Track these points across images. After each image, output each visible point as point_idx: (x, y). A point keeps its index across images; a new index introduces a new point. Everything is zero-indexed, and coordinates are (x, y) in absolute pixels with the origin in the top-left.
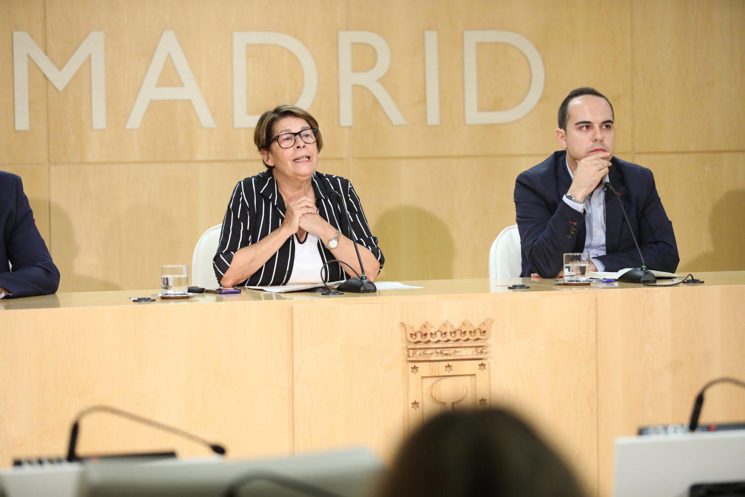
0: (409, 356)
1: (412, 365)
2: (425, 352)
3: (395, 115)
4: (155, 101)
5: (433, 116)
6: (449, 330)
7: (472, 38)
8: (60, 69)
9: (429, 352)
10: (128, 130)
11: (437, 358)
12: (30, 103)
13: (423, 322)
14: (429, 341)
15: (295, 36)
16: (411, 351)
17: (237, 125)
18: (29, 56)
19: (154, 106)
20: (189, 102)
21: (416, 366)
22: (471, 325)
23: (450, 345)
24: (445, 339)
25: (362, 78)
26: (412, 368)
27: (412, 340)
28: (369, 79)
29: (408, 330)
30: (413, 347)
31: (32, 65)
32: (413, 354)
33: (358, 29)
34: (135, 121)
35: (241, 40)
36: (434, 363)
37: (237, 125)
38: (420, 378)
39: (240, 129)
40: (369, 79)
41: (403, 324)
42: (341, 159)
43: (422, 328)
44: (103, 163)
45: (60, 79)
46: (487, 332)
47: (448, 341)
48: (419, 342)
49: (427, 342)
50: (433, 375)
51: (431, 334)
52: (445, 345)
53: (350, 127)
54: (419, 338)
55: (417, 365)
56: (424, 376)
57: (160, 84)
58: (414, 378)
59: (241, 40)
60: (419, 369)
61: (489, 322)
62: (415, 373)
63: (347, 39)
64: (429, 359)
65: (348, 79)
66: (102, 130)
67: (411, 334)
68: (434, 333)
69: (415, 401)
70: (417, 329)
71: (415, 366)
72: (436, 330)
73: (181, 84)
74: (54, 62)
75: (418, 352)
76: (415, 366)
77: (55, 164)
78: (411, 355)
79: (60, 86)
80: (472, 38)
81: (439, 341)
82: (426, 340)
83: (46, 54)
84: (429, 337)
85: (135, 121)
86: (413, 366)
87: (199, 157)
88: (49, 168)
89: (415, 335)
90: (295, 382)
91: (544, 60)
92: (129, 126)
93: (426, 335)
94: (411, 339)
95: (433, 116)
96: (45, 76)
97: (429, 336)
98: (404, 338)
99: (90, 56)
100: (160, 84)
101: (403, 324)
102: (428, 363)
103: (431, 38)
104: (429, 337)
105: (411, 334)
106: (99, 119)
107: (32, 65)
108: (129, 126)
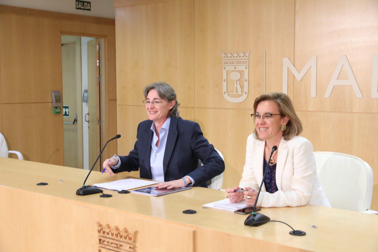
4: (337, 85)
6: (115, 232)
10: (325, 98)
11: (109, 248)
20: (351, 86)
21: (101, 249)
23: (115, 242)
24: (113, 237)
32: (100, 242)
34: (327, 95)
36: (108, 250)
39: (374, 98)
44: (315, 111)
55: (102, 249)
61: (133, 233)
66: (314, 97)
67: (99, 232)
68: (108, 232)
72: (109, 231)
85: (327, 95)
87: (355, 111)
92: (324, 97)
96: (294, 75)
97: (106, 234)
106: (313, 94)
108: (324, 97)
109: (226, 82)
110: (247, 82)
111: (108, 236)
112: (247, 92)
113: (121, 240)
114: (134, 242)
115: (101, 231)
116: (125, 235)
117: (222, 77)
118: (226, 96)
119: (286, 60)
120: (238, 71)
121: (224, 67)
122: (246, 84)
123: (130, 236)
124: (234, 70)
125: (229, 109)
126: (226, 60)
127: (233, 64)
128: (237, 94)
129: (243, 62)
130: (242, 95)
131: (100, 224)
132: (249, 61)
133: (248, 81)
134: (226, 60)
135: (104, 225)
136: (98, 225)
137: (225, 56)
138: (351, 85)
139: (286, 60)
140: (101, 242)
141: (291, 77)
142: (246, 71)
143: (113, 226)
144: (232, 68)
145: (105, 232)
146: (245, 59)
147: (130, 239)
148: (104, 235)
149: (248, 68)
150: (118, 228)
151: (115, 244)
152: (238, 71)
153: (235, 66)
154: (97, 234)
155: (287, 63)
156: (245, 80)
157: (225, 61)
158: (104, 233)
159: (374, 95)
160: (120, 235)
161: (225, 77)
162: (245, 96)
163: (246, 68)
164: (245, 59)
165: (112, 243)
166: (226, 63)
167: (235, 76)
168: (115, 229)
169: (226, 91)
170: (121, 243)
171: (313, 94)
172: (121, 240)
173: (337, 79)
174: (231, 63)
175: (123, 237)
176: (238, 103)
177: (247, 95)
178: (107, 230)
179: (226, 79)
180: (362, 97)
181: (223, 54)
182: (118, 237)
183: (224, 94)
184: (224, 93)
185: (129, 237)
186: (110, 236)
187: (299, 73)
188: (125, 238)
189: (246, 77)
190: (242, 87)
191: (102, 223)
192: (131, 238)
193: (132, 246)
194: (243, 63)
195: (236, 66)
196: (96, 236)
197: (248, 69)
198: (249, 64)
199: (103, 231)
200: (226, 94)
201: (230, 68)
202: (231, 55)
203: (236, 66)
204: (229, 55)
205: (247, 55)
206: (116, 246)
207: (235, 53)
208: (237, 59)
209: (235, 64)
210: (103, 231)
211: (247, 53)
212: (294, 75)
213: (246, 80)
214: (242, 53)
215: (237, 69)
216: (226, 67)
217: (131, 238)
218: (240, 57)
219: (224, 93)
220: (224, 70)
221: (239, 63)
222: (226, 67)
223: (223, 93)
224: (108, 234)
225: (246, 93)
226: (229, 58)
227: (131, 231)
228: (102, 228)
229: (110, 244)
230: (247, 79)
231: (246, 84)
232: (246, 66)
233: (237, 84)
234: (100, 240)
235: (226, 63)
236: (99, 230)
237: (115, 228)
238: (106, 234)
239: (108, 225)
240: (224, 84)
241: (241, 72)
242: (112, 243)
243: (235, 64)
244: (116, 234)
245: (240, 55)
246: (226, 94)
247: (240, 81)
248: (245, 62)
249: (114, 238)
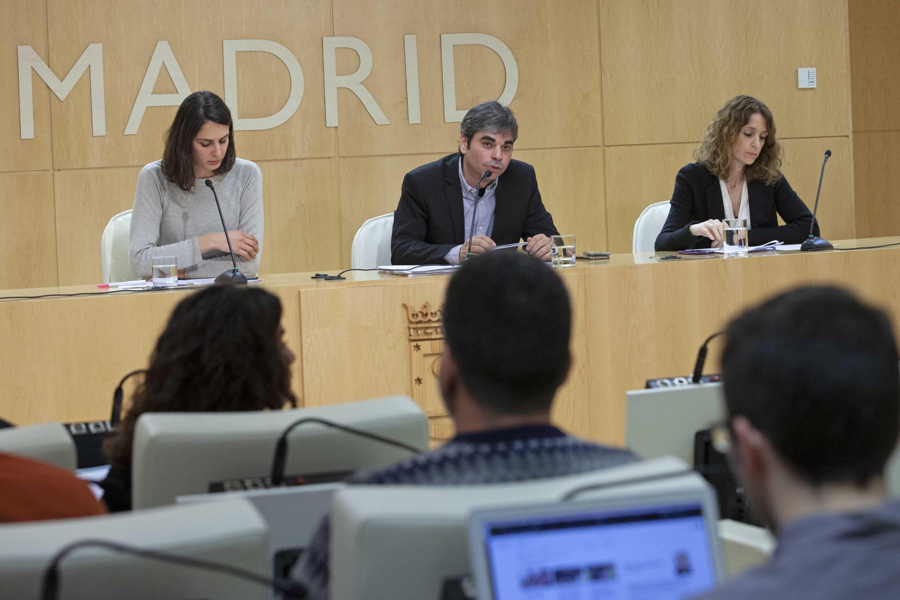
0: (410, 335)
1: (414, 344)
2: (426, 331)
3: (379, 116)
5: (415, 116)
7: (449, 41)
8: (62, 82)
9: (429, 331)
10: (126, 135)
12: (34, 112)
13: (423, 303)
14: (430, 321)
15: (282, 44)
16: (412, 330)
19: (150, 111)
21: (418, 344)
25: (346, 81)
26: (414, 346)
27: (414, 320)
28: (353, 82)
29: (409, 310)
30: (414, 326)
31: (36, 75)
33: (341, 35)
35: (231, 48)
36: (435, 341)
38: (422, 356)
40: (353, 82)
41: (405, 306)
42: (329, 158)
43: (422, 308)
44: (103, 168)
45: (62, 89)
48: (420, 322)
49: (426, 322)
50: (435, 352)
51: (432, 314)
53: (335, 127)
54: (420, 318)
55: (419, 343)
56: (426, 353)
57: (154, 92)
58: (416, 355)
59: (231, 48)
60: (421, 347)
62: (417, 351)
63: (331, 44)
65: (333, 82)
67: (413, 315)
68: (434, 312)
69: (418, 378)
70: (418, 309)
71: (417, 344)
72: (436, 310)
74: (56, 74)
75: (420, 332)
76: (417, 344)
78: (412, 334)
80: (449, 41)
82: (427, 319)
83: (49, 67)
84: (429, 317)
85: (132, 128)
86: (415, 345)
88: (53, 173)
89: (417, 315)
90: (305, 363)
91: (517, 60)
93: (426, 315)
94: (413, 319)
95: (415, 116)
96: (47, 86)
97: (429, 315)
98: (406, 320)
99: (90, 66)
100: (154, 92)
101: (405, 306)
102: (430, 341)
103: (411, 40)
104: (429, 317)
105: (413, 315)
106: (100, 127)
107: (36, 75)
119: (25, 51)
139: (25, 51)
171: (100, 127)
173: (152, 94)
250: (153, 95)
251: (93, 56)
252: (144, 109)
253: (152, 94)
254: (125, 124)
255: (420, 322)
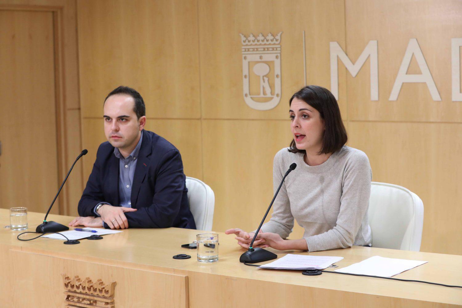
6: (87, 285)
10: (391, 101)
12: (338, 85)
17: (454, 99)
18: (338, 57)
19: (404, 85)
22: (102, 283)
23: (88, 297)
24: (84, 292)
34: (393, 96)
37: (454, 99)
39: (456, 102)
45: (353, 70)
46: (110, 292)
47: (86, 294)
48: (69, 291)
51: (78, 287)
52: (85, 296)
64: (76, 305)
67: (66, 285)
72: (79, 283)
73: (420, 73)
77: (353, 121)
79: (354, 74)
81: (81, 293)
85: (393, 96)
87: (432, 120)
96: (346, 68)
97: (75, 288)
106: (374, 95)
109: (247, 79)
110: (279, 79)
111: (78, 291)
112: (280, 93)
113: (95, 294)
114: (112, 296)
115: (69, 285)
116: (100, 287)
117: (242, 71)
118: (248, 101)
120: (266, 62)
121: (244, 56)
122: (277, 82)
123: (107, 289)
124: (260, 60)
125: (253, 120)
126: (247, 45)
127: (257, 52)
128: (266, 98)
129: (272, 48)
130: (272, 98)
131: (67, 276)
132: (281, 46)
133: (280, 76)
134: (247, 45)
135: (72, 277)
136: (65, 277)
137: (245, 39)
138: (425, 83)
139: (334, 46)
140: (70, 299)
141: (342, 70)
142: (277, 62)
143: (83, 279)
144: (256, 58)
145: (74, 285)
146: (274, 44)
147: (107, 292)
148: (73, 290)
149: (279, 57)
150: (90, 279)
151: (88, 300)
152: (266, 62)
153: (259, 55)
154: (63, 289)
155: (336, 50)
156: (275, 76)
157: (245, 47)
158: (72, 286)
159: (456, 96)
160: (94, 288)
161: (245, 72)
162: (276, 100)
163: (277, 57)
164: (274, 44)
165: (84, 299)
166: (247, 50)
167: (261, 70)
168: (87, 282)
169: (248, 93)
170: (96, 299)
171: (374, 95)
172: (95, 294)
173: (407, 74)
174: (254, 50)
175: (98, 290)
176: (266, 111)
177: (279, 98)
178: (77, 284)
179: (247, 75)
180: (440, 100)
181: (242, 36)
182: (91, 291)
183: (245, 98)
184: (246, 95)
185: (105, 290)
186: (81, 290)
187: (354, 64)
188: (101, 291)
189: (277, 71)
190: (272, 86)
191: (69, 276)
192: (108, 291)
193: (109, 301)
194: (272, 50)
195: (262, 55)
196: (63, 292)
197: (279, 60)
198: (281, 52)
199: (71, 285)
200: (249, 96)
201: (253, 57)
202: (253, 38)
203: (262, 55)
204: (251, 38)
205: (278, 37)
206: (88, 302)
207: (260, 35)
208: (263, 43)
209: (261, 52)
210: (71, 285)
211: (277, 35)
212: (348, 68)
213: (277, 76)
214: (270, 35)
215: (263, 60)
216: (246, 55)
217: (108, 291)
218: (267, 41)
219: (246, 95)
220: (244, 60)
221: (266, 49)
222: (246, 55)
223: (244, 95)
224: (78, 287)
225: (277, 95)
226: (251, 43)
227: (107, 284)
228: (69, 281)
229: (81, 300)
230: (279, 74)
231: (277, 82)
232: (276, 55)
233: (264, 82)
234: (68, 296)
235: (247, 50)
236: (67, 284)
237: (87, 279)
238: (75, 289)
239: (78, 277)
240: (246, 82)
241: (270, 64)
242: (84, 299)
243: (261, 52)
244: (88, 288)
245: (267, 38)
246: (249, 96)
247: (269, 76)
248: (275, 49)
249: (86, 293)
250: (408, 75)
251: (371, 49)
252: (401, 84)
253: (407, 74)
254: (390, 93)
255: (69, 291)
